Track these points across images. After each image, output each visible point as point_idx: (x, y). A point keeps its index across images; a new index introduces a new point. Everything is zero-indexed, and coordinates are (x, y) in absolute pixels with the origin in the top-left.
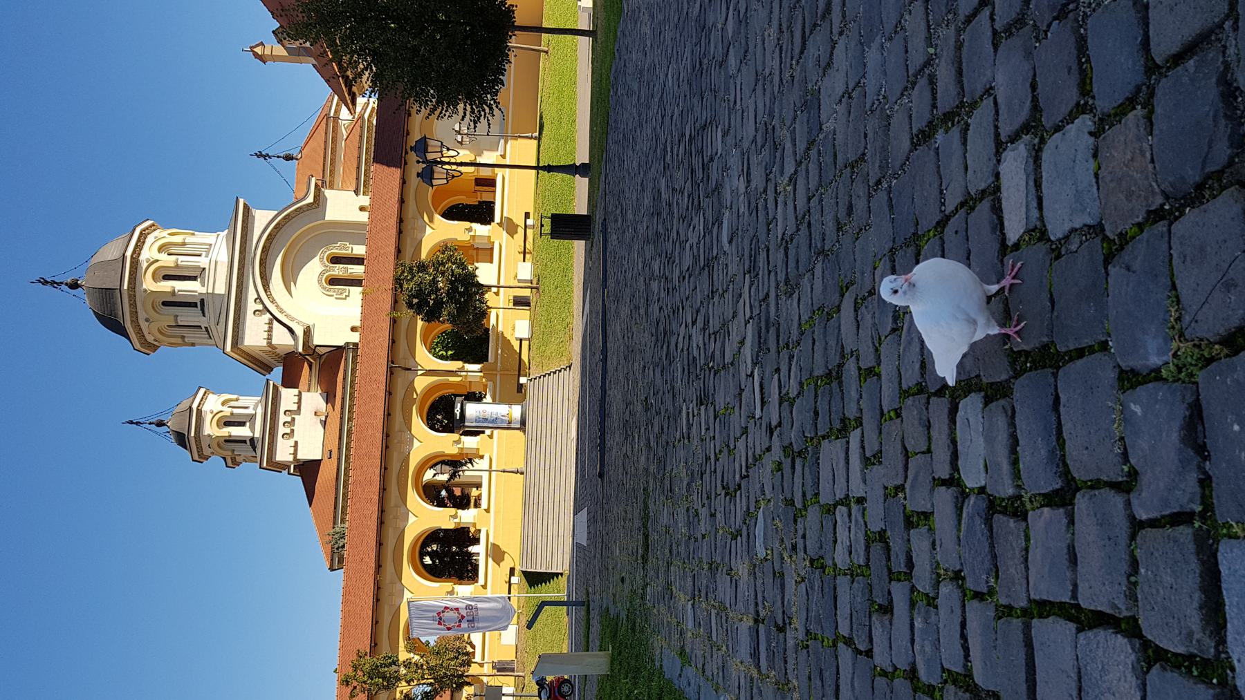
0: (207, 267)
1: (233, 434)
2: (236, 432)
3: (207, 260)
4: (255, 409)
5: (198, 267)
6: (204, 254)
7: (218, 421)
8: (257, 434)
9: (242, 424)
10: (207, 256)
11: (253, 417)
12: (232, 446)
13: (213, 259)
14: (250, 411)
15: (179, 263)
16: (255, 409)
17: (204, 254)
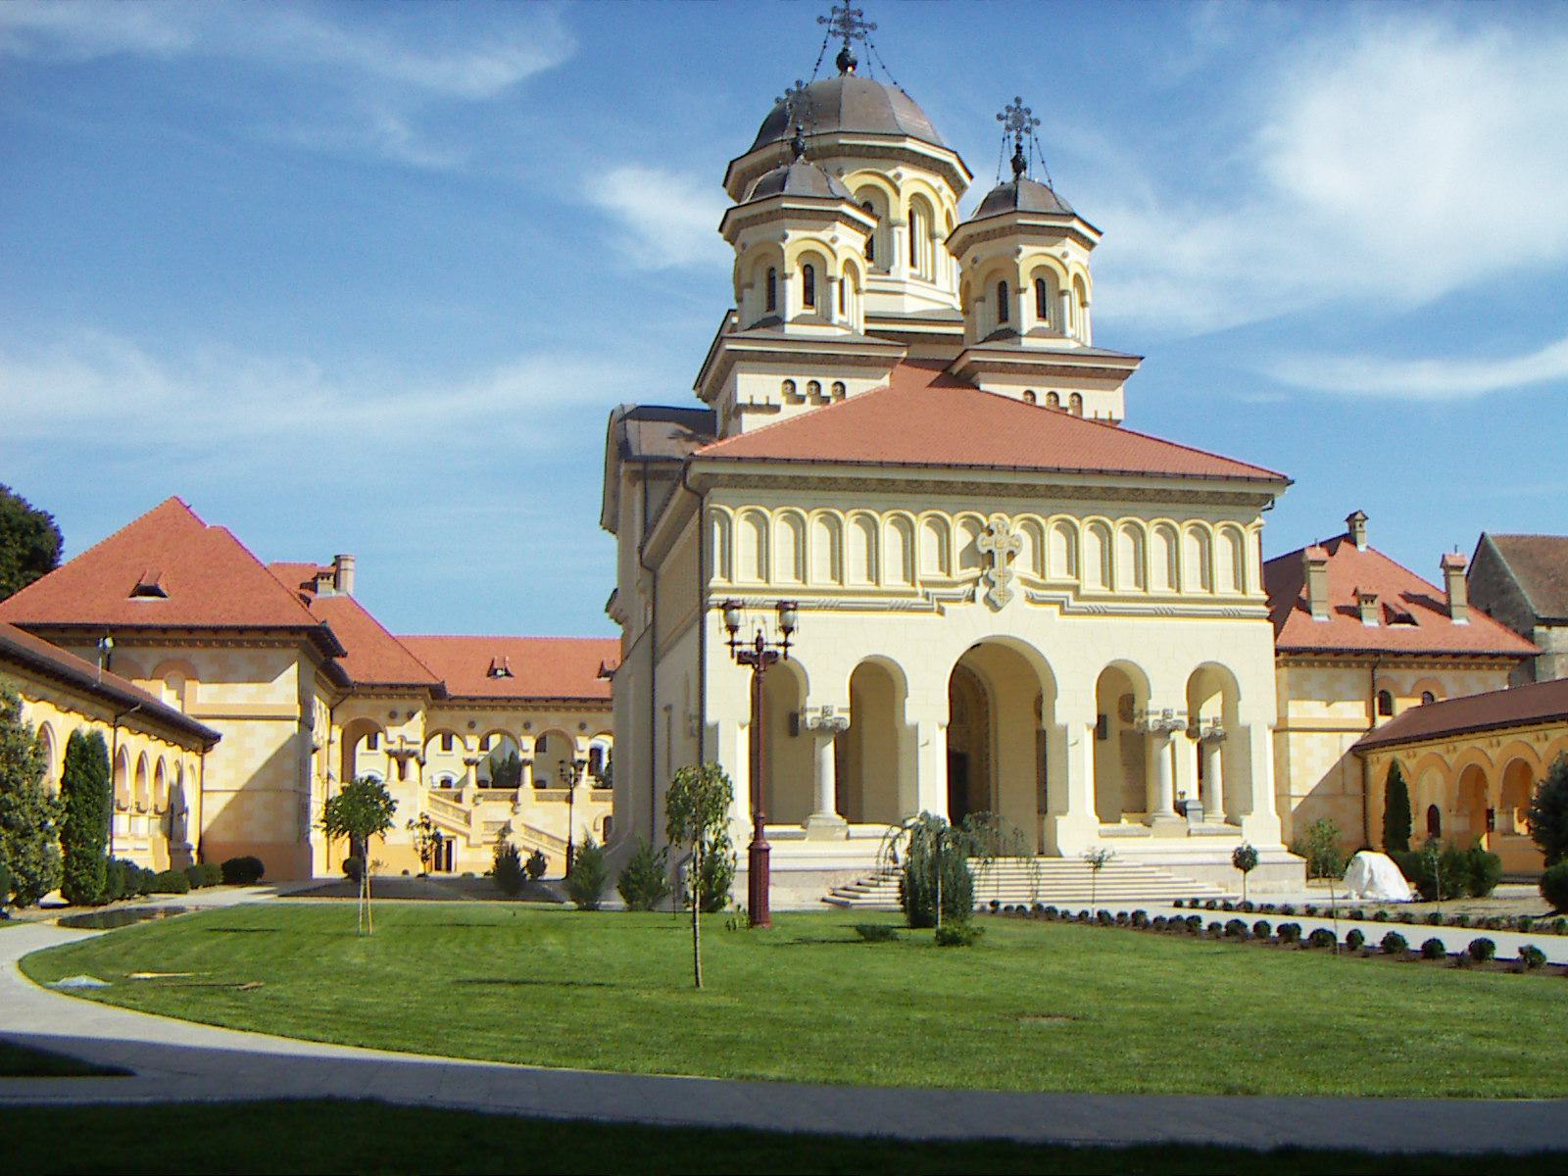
0: (891, 277)
1: (789, 283)
2: (794, 289)
3: (905, 277)
4: (842, 325)
5: (891, 262)
6: (916, 272)
7: (817, 253)
8: (791, 330)
9: (809, 300)
10: (912, 276)
11: (826, 320)
12: (761, 286)
13: (908, 288)
14: (837, 317)
15: (896, 229)
16: (842, 325)
17: (916, 272)
